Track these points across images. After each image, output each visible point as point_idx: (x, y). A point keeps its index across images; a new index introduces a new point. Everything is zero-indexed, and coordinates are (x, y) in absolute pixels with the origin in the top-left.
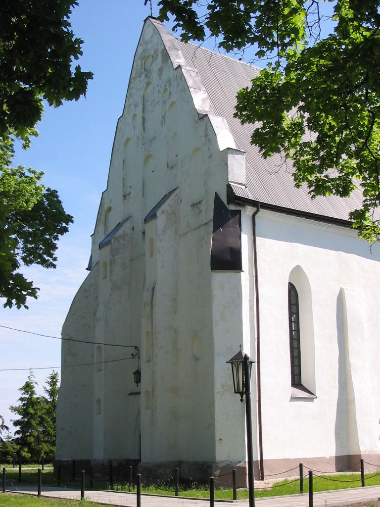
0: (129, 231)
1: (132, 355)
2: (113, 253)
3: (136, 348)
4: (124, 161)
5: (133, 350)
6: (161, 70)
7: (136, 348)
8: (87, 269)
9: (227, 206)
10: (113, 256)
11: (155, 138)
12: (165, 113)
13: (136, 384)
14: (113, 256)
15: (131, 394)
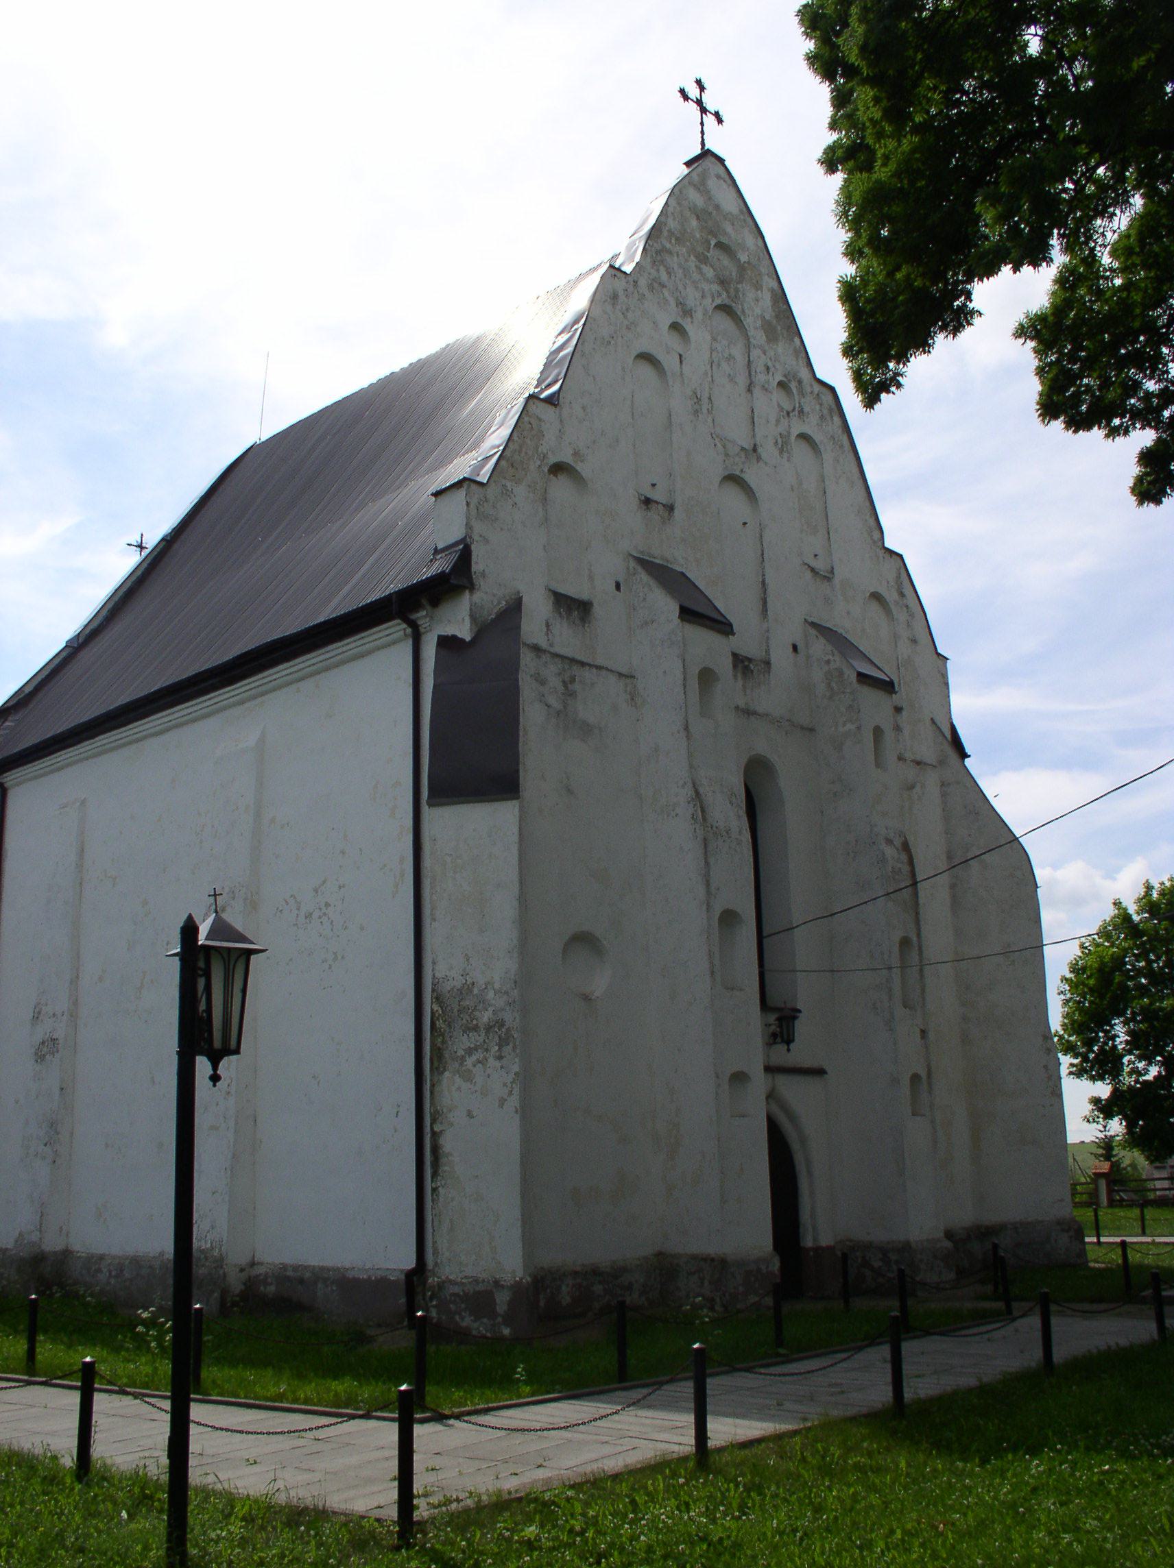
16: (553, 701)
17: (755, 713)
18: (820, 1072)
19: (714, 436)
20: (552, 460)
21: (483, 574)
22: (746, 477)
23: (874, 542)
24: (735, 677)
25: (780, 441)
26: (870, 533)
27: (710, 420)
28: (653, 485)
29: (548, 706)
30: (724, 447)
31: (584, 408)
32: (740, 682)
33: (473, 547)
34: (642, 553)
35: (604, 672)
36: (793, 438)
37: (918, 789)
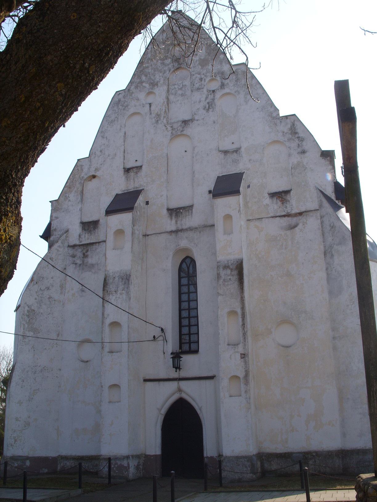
0: (143, 204)
1: (154, 337)
2: (134, 222)
3: (162, 330)
4: (125, 134)
5: (158, 332)
6: (203, 63)
7: (162, 330)
8: (40, 236)
9: (337, 202)
10: (134, 226)
11: (192, 120)
12: (213, 99)
13: (175, 369)
14: (134, 226)
15: (146, 380)
16: (79, 262)
17: (182, 230)
18: (212, 378)
19: (166, 125)
20: (86, 177)
21: (55, 230)
22: (184, 132)
23: (274, 118)
24: (171, 219)
25: (207, 106)
26: (270, 115)
27: (165, 119)
28: (136, 161)
29: (76, 264)
30: (172, 127)
31: (101, 151)
32: (174, 221)
33: (52, 223)
34: (124, 191)
35: (101, 244)
36: (216, 101)
37: (300, 226)
